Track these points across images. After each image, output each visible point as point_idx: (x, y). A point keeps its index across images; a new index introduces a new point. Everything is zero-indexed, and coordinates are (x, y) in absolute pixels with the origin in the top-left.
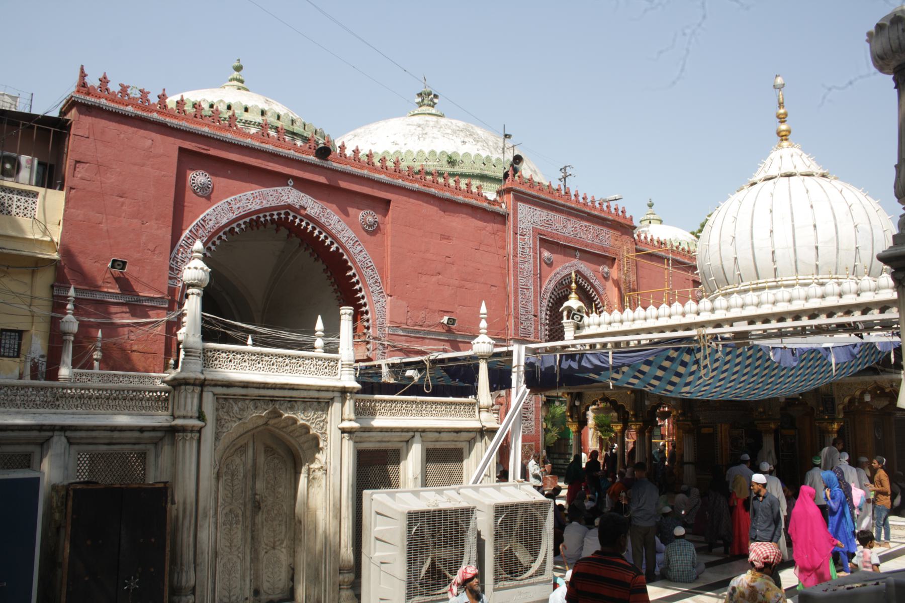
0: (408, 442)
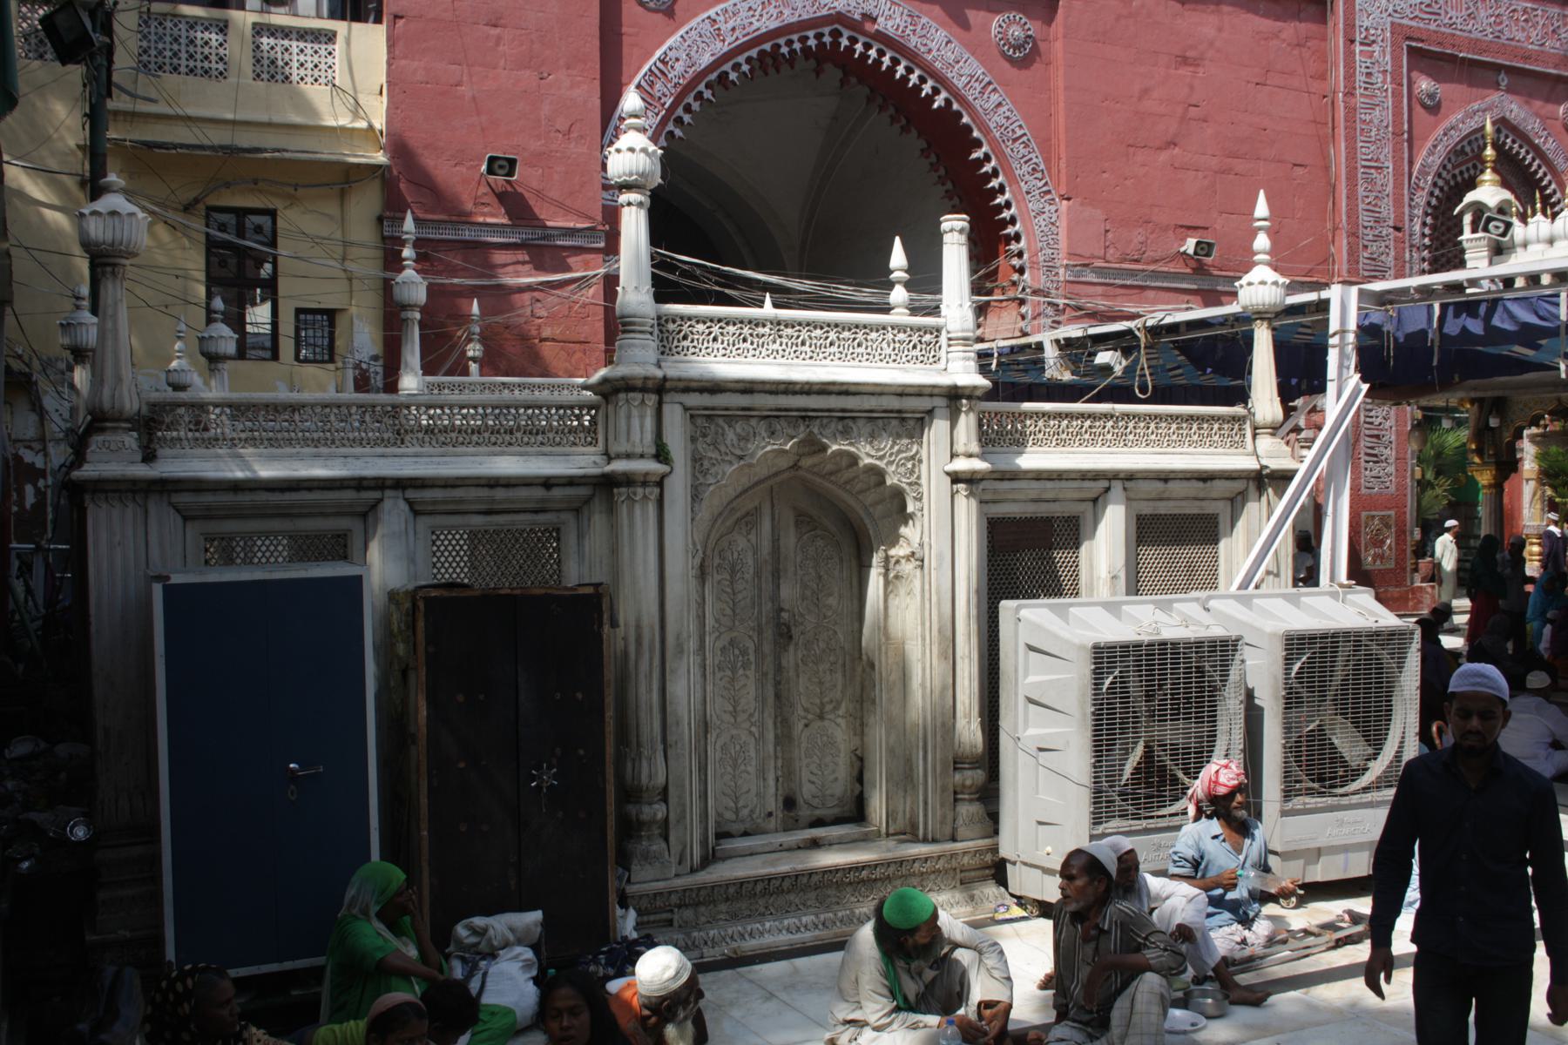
0: (1097, 502)
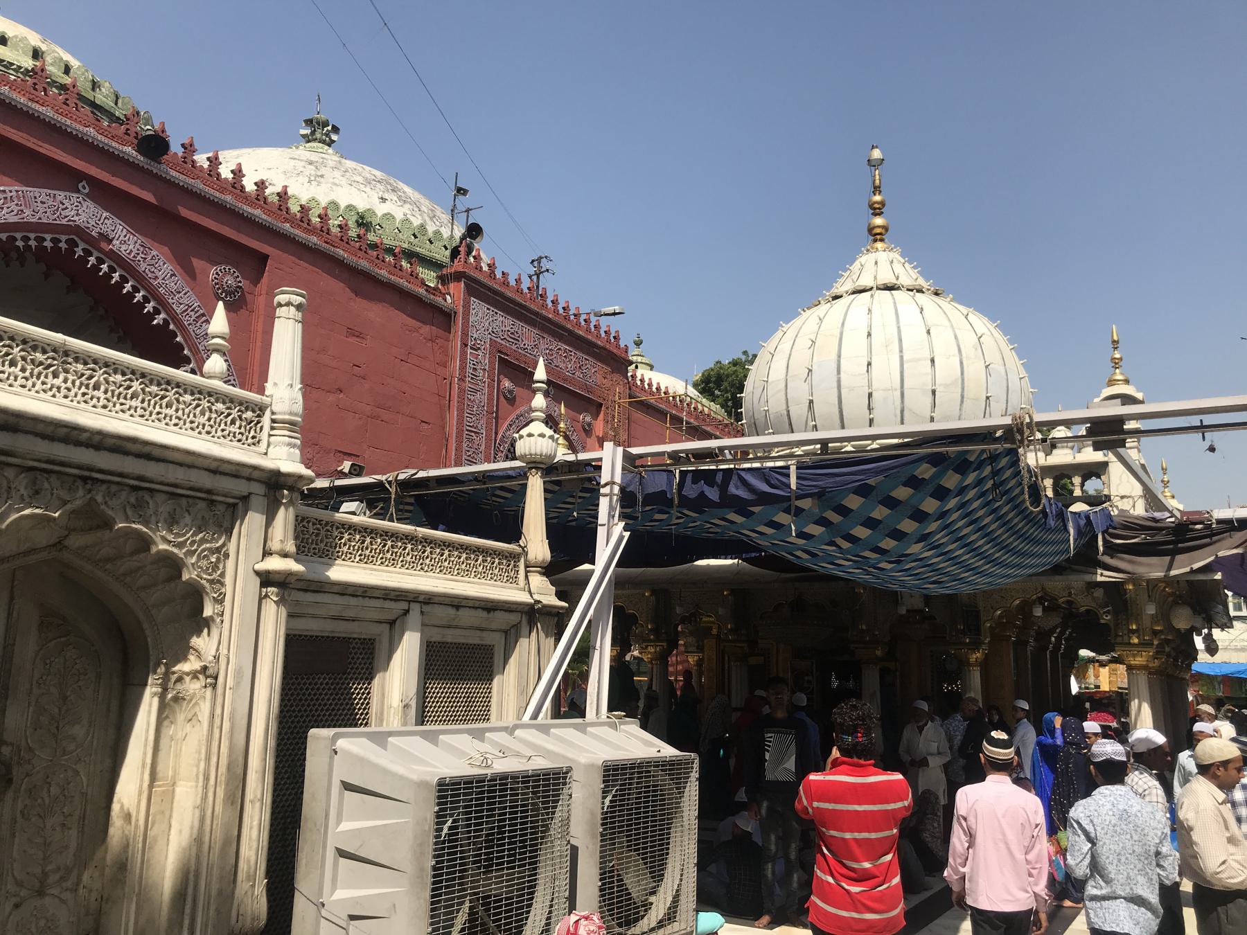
0: (395, 626)
